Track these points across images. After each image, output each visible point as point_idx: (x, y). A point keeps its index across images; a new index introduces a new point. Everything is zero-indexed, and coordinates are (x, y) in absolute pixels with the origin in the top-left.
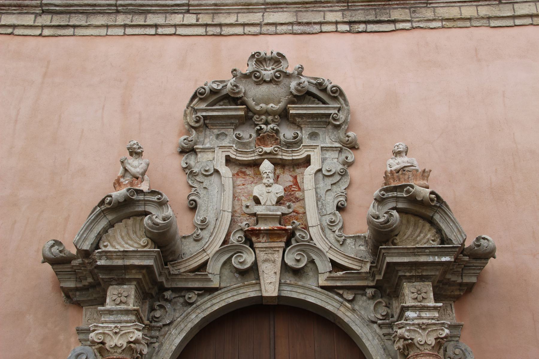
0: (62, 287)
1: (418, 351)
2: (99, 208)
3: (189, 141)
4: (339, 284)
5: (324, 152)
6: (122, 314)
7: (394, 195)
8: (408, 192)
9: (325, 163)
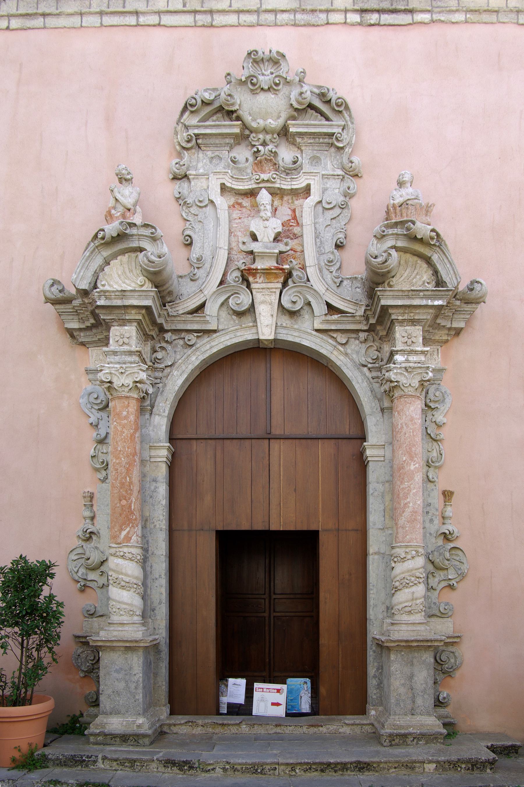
0: (67, 328)
1: (403, 393)
2: (92, 244)
3: (181, 166)
4: (333, 327)
5: (326, 180)
6: (126, 355)
7: (394, 232)
8: (408, 229)
9: (326, 193)
